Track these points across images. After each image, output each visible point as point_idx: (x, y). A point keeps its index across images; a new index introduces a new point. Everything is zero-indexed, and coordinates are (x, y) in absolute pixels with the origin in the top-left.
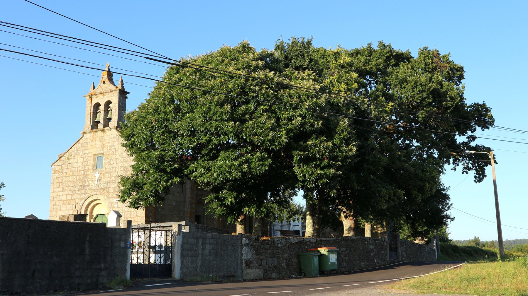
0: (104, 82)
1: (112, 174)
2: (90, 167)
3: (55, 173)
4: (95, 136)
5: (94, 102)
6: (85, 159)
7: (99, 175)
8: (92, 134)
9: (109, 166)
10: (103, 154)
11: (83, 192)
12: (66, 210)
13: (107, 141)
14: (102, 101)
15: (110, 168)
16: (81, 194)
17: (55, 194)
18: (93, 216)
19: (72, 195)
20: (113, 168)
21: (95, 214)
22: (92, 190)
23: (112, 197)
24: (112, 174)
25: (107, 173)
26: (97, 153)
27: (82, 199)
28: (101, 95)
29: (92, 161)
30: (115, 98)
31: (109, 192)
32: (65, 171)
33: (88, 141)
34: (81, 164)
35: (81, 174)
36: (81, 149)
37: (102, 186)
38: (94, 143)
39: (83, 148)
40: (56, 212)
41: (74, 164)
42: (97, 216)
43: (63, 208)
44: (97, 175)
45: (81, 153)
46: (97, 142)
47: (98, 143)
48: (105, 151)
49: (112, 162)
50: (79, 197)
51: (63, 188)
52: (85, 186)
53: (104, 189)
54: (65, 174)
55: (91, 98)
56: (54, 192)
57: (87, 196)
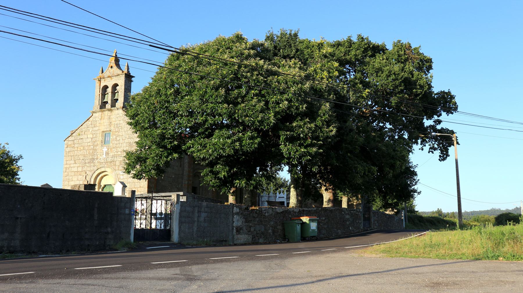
0: (112, 67)
1: (118, 149)
2: (99, 143)
3: (67, 147)
4: (103, 115)
5: (103, 84)
6: (94, 136)
8: (100, 113)
9: (116, 142)
10: (110, 131)
11: (92, 164)
12: (78, 180)
13: (114, 120)
15: (117, 144)
16: (90, 166)
18: (101, 186)
19: (82, 167)
21: (103, 184)
22: (101, 163)
23: (118, 170)
24: (118, 149)
26: (105, 130)
30: (121, 81)
31: (115, 165)
32: (76, 146)
37: (109, 160)
38: (102, 121)
39: (93, 126)
40: (68, 182)
41: (84, 140)
42: (105, 185)
43: (75, 178)
44: (105, 149)
45: (91, 130)
47: (106, 122)
48: (112, 128)
49: (118, 139)
50: (89, 169)
51: (75, 161)
52: (94, 159)
53: (111, 162)
54: (76, 149)
55: (100, 81)
57: (96, 168)
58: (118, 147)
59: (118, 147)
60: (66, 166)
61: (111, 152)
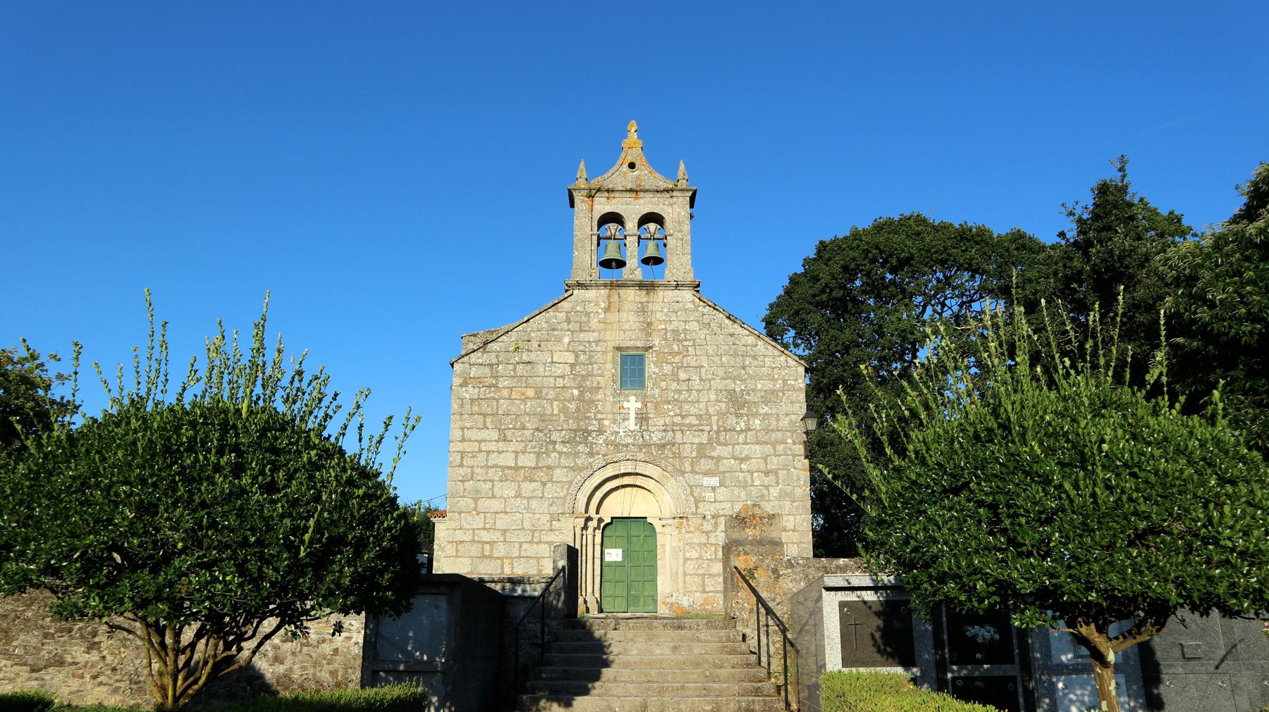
0: (632, 166)
1: (686, 407)
4: (615, 298)
5: (603, 206)
6: (582, 358)
7: (639, 405)
14: (632, 210)
15: (679, 392)
17: (468, 447)
19: (538, 455)
20: (689, 390)
21: (607, 514)
23: (693, 472)
25: (668, 403)
26: (631, 344)
27: (580, 469)
28: (628, 195)
29: (609, 366)
31: (679, 457)
32: (503, 383)
33: (591, 307)
34: (568, 368)
35: (568, 395)
36: (565, 326)
38: (613, 317)
39: (576, 327)
40: (476, 500)
44: (632, 404)
45: (566, 340)
46: (624, 315)
47: (630, 319)
49: (683, 375)
53: (664, 446)
55: (591, 196)
56: (463, 440)
58: (686, 401)
59: (686, 401)
60: (460, 446)
61: (659, 412)
